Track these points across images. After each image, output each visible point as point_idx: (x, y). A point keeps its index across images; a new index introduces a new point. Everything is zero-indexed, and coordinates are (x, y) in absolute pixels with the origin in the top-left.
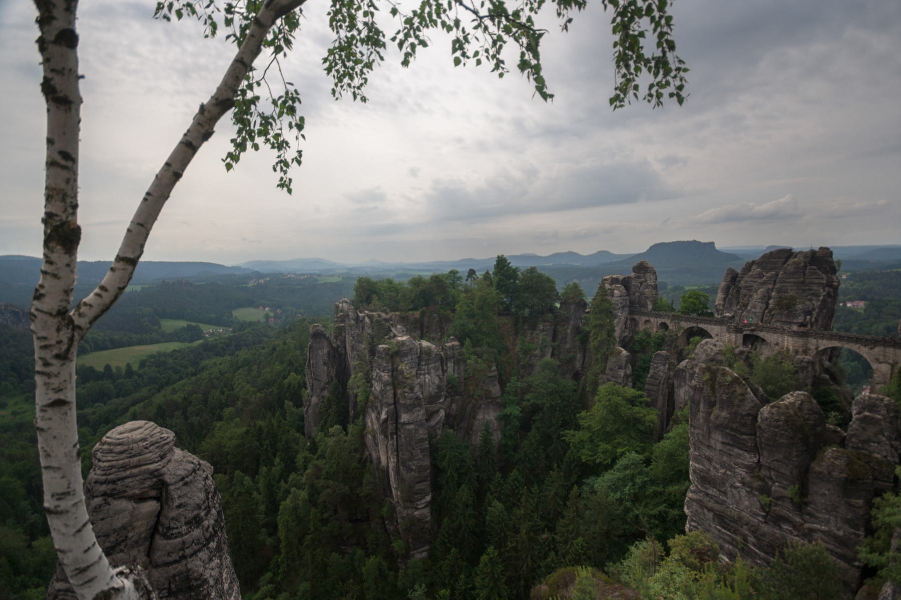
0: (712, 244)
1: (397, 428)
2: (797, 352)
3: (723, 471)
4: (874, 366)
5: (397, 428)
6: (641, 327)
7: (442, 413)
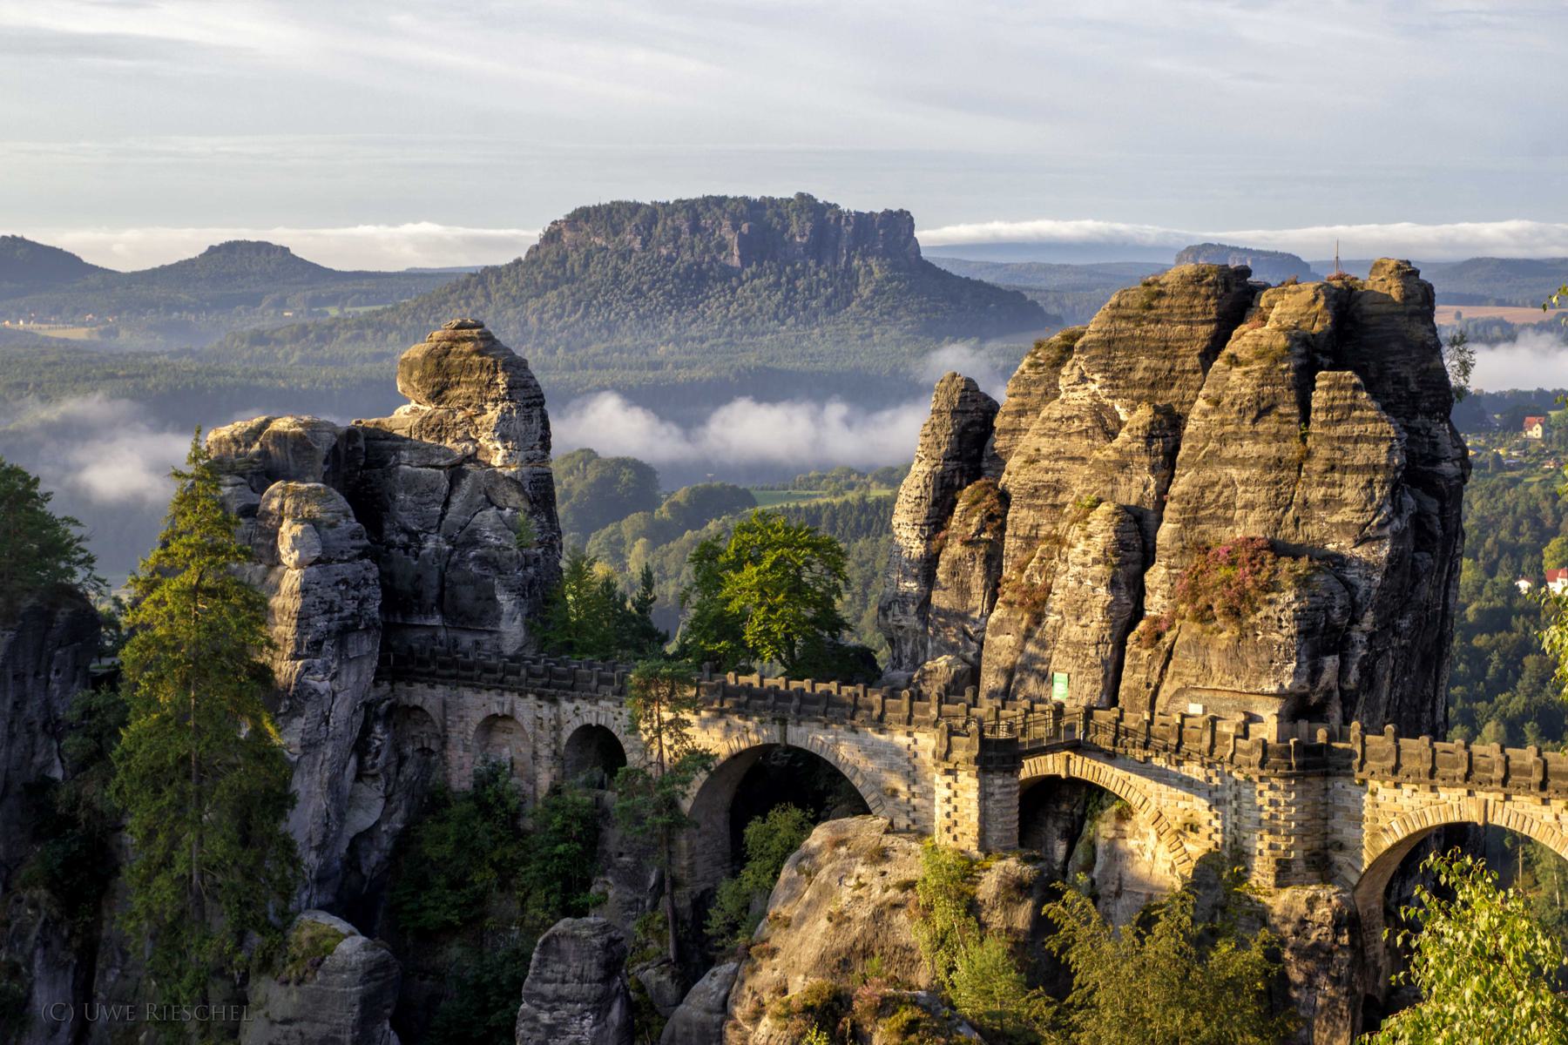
6: (461, 767)
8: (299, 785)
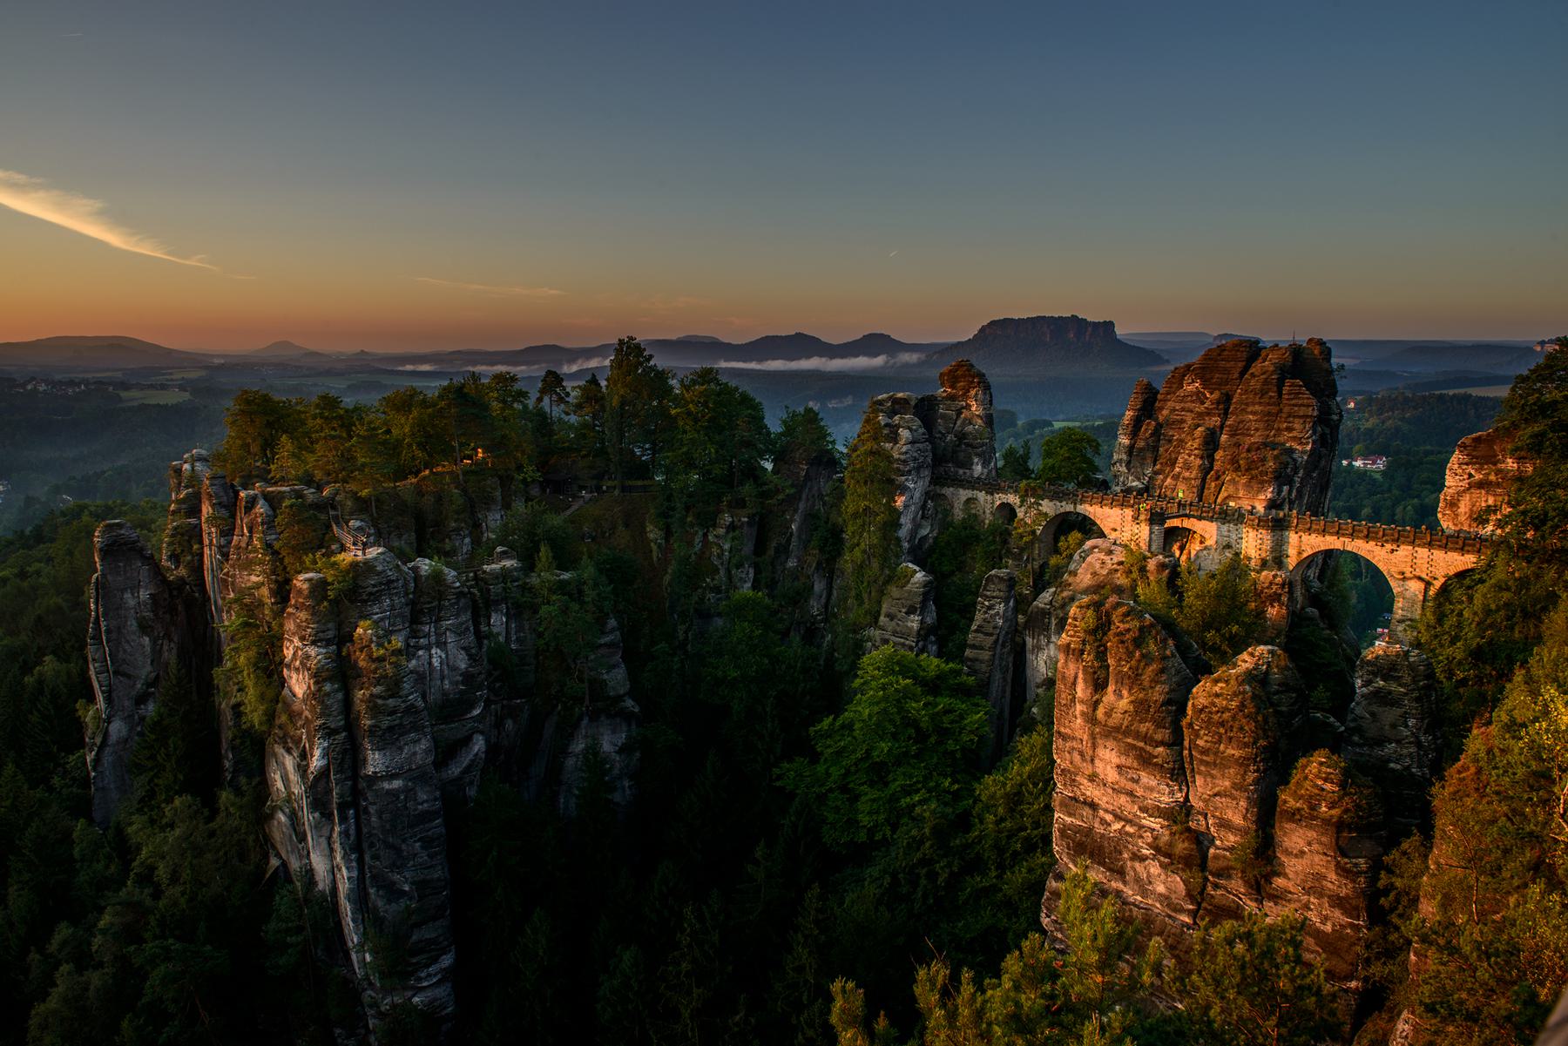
0: (1108, 326)
1: (356, 793)
2: (1264, 564)
3: (1117, 826)
4: (1396, 587)
5: (356, 793)
7: (479, 744)
8: (902, 520)
